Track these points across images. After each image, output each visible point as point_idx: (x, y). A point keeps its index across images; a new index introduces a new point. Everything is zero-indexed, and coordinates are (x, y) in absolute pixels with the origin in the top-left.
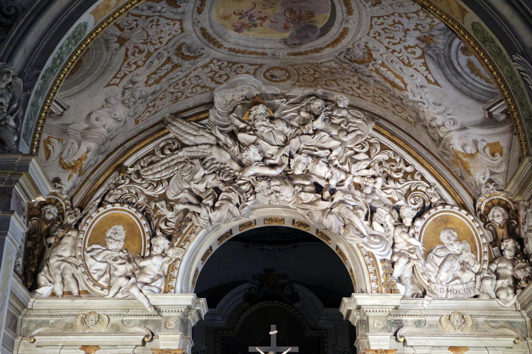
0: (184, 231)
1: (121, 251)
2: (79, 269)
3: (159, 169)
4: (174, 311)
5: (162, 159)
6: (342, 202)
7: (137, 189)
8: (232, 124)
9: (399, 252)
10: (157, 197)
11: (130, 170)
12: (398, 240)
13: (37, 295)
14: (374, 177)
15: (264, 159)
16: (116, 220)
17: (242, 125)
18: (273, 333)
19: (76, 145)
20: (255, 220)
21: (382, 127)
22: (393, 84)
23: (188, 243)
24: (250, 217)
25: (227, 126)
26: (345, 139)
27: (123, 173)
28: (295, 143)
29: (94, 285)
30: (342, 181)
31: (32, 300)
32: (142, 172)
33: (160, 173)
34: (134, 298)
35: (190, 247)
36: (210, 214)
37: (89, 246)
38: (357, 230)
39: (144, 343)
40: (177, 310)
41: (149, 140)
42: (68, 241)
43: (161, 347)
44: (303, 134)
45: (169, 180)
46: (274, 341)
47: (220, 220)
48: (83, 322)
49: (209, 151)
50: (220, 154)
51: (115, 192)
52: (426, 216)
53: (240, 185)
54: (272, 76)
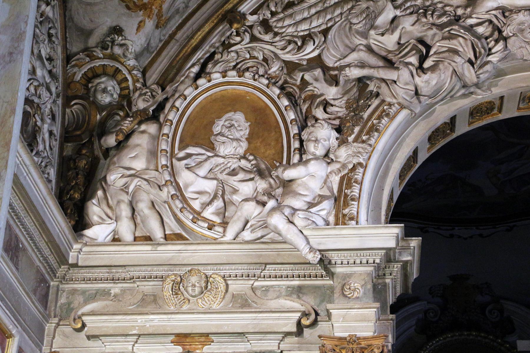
0: (366, 115)
1: (244, 157)
2: (165, 189)
3: (306, 15)
4: (358, 261)
7: (266, 52)
10: (305, 63)
11: (252, 19)
13: (85, 239)
20: (502, 98)
23: (376, 134)
24: (493, 89)
27: (238, 23)
31: (76, 246)
32: (272, 21)
33: (308, 21)
35: (382, 142)
36: (417, 80)
37: (181, 149)
39: (300, 328)
40: (364, 261)
42: (141, 141)
43: (338, 334)
45: (325, 32)
51: (225, 57)
53: (472, 26)
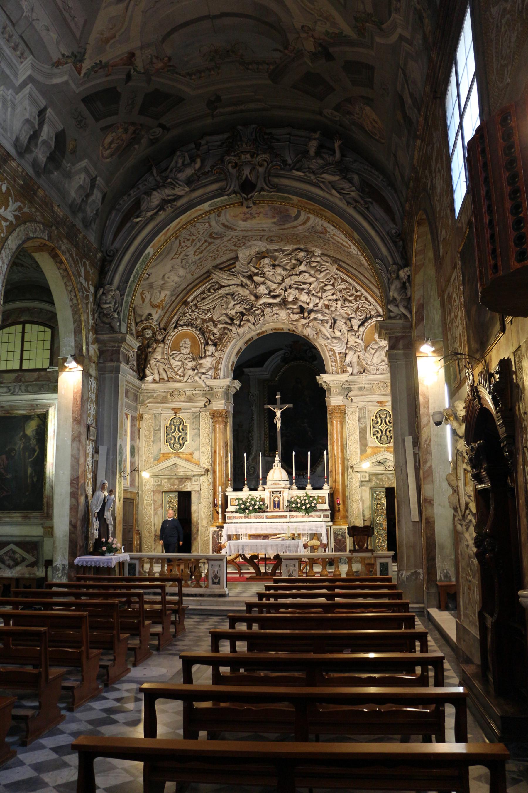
5: (210, 296)
6: (315, 319)
8: (250, 270)
9: (350, 347)
11: (191, 304)
12: (350, 339)
14: (336, 300)
15: (270, 292)
16: (185, 336)
17: (256, 271)
18: (278, 397)
19: (158, 294)
21: (342, 267)
22: (342, 244)
25: (247, 272)
26: (319, 276)
28: (288, 281)
29: (176, 375)
30: (317, 304)
34: (197, 382)
38: (325, 335)
39: (205, 406)
41: (201, 284)
42: (159, 350)
43: (214, 409)
44: (293, 275)
45: (214, 308)
46: (278, 402)
47: (244, 333)
48: (172, 395)
49: (237, 289)
50: (244, 291)
52: (366, 324)
53: (255, 311)
54: (272, 240)
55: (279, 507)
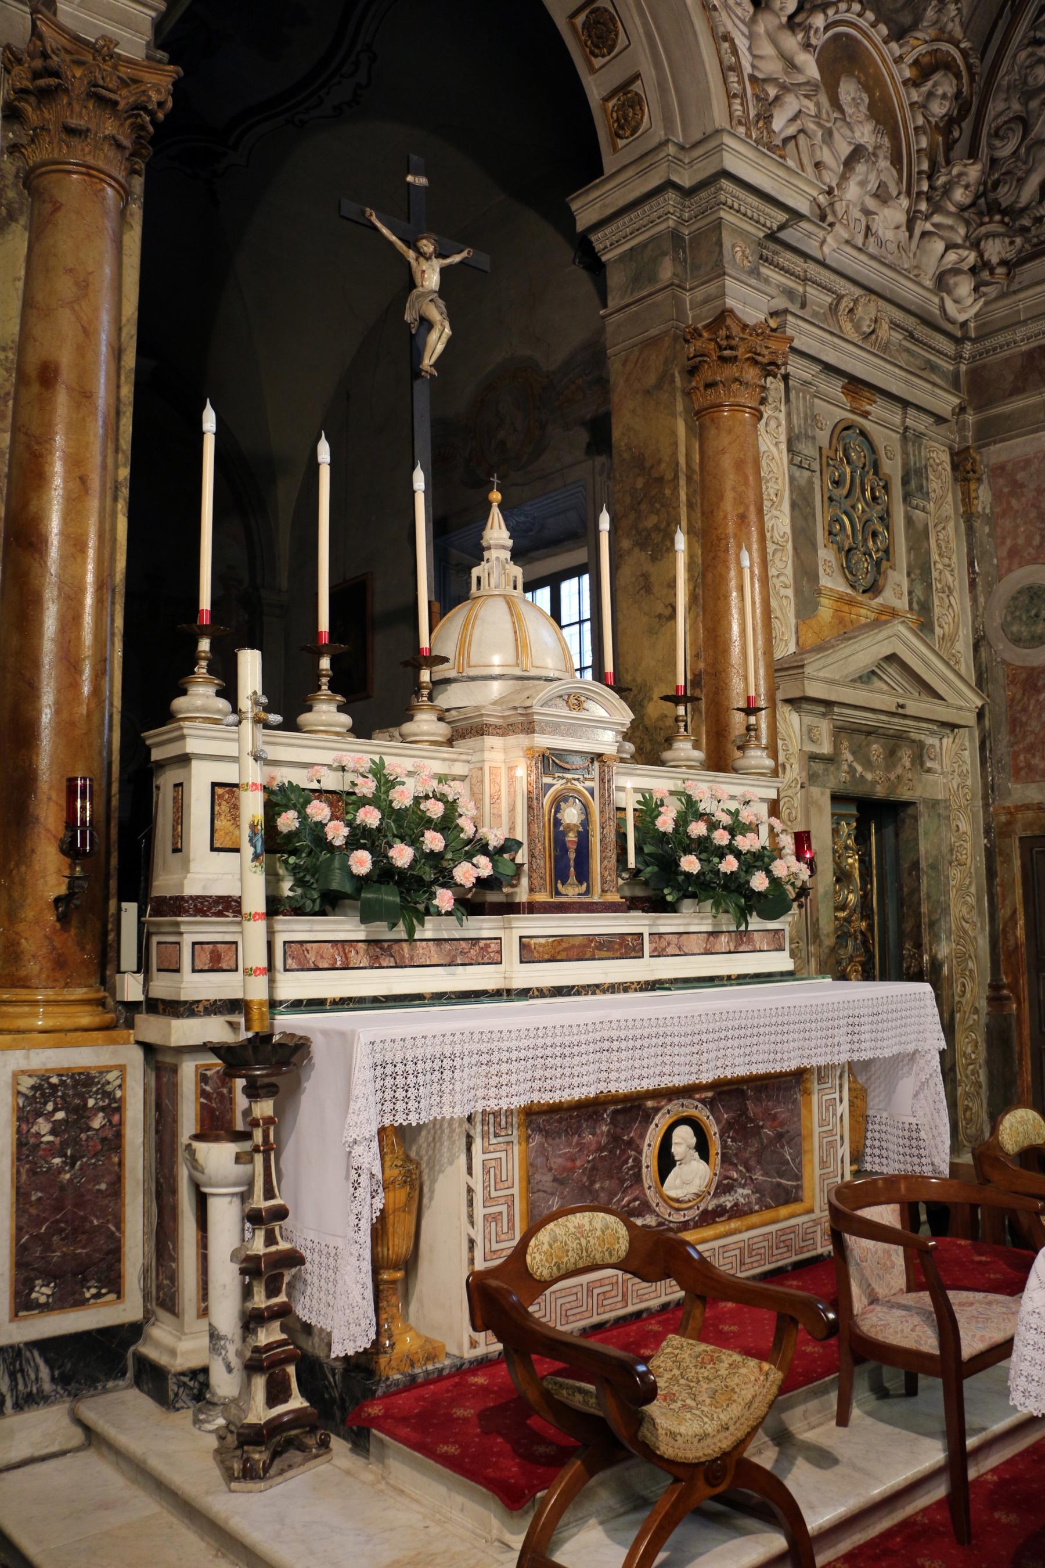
55: (583, 875)
